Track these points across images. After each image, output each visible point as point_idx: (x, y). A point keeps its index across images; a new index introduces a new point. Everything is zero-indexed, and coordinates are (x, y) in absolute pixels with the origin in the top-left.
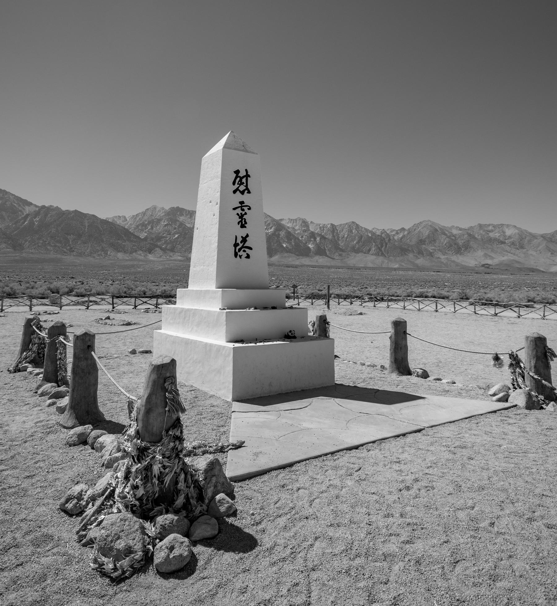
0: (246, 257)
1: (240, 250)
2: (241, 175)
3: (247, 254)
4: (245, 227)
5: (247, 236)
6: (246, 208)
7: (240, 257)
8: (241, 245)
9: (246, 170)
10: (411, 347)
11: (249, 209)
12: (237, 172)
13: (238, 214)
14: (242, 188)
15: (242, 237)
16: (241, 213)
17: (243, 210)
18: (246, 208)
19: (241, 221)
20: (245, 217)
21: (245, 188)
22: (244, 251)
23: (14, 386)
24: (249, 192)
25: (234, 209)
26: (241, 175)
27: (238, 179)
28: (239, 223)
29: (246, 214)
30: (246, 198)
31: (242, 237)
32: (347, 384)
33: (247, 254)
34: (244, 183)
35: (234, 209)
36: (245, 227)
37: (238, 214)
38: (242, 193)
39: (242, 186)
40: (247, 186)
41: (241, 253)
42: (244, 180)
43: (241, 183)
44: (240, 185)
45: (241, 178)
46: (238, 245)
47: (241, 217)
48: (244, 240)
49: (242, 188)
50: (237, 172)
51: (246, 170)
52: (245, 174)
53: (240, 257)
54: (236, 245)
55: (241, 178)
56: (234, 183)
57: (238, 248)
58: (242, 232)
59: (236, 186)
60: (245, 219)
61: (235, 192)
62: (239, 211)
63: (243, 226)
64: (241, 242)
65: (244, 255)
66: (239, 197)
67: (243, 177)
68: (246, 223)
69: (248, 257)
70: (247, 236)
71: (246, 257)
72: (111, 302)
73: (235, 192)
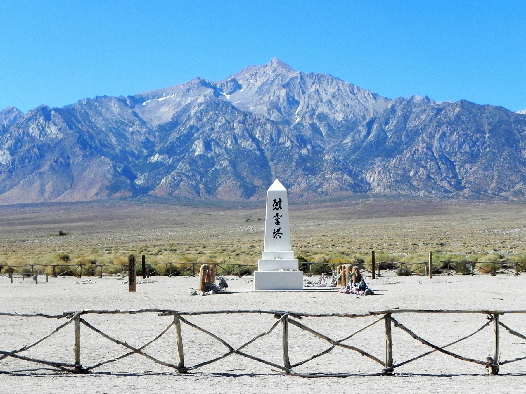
2: (277, 201)
12: (275, 200)
14: (277, 207)
23: (150, 253)
24: (281, 208)
26: (277, 201)
30: (280, 212)
38: (278, 209)
42: (278, 204)
43: (277, 205)
45: (277, 203)
47: (277, 220)
48: (278, 230)
49: (277, 207)
50: (275, 200)
54: (274, 233)
55: (277, 203)
56: (273, 206)
59: (275, 206)
61: (274, 209)
62: (276, 218)
63: (278, 224)
66: (276, 211)
69: (280, 238)
73: (274, 209)
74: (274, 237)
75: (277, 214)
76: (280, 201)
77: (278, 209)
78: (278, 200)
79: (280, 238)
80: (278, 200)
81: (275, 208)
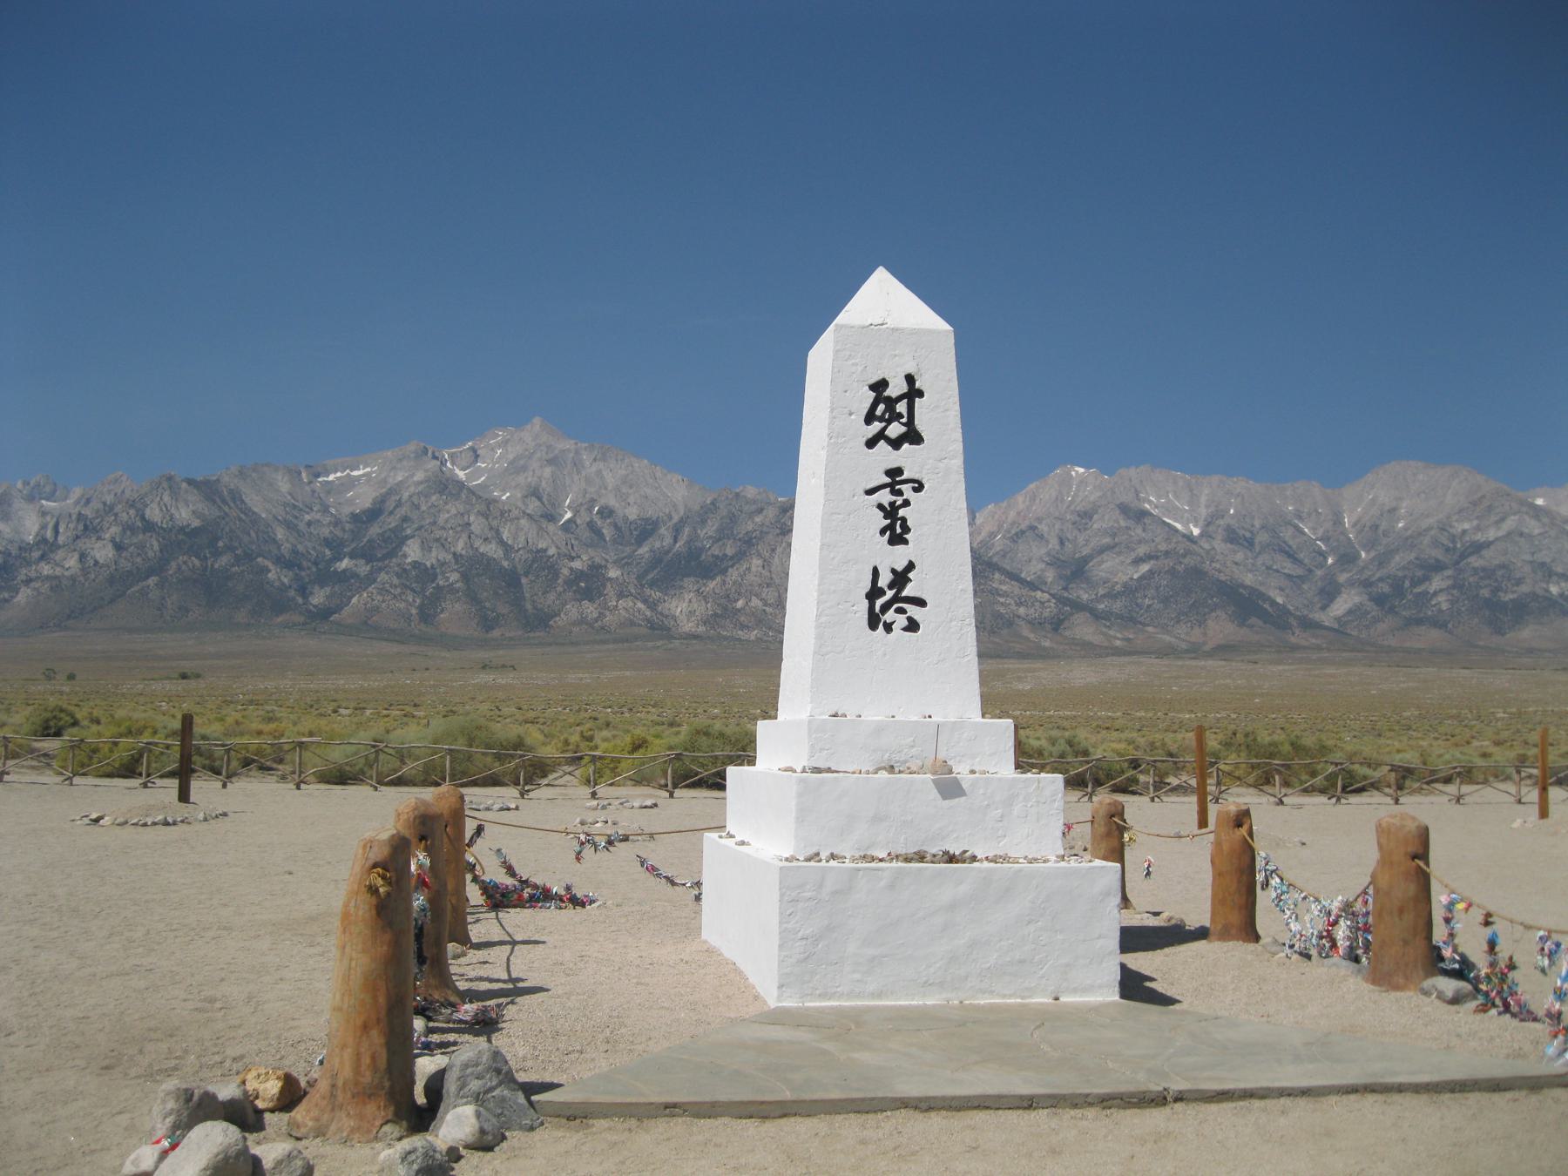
0: (905, 629)
1: (885, 608)
2: (893, 391)
3: (910, 619)
4: (906, 542)
5: (911, 566)
6: (905, 488)
7: (888, 628)
8: (890, 594)
9: (910, 379)
10: (1519, 1055)
11: (919, 487)
12: (880, 386)
13: (880, 507)
14: (895, 430)
15: (893, 571)
16: (892, 504)
17: (900, 493)
18: (905, 488)
19: (891, 527)
20: (901, 512)
21: (903, 429)
22: (901, 611)
25: (870, 492)
26: (893, 391)
27: (881, 407)
28: (883, 532)
29: (906, 503)
30: (907, 457)
31: (893, 571)
32: (720, 1121)
33: (910, 619)
34: (900, 416)
35: (870, 492)
36: (906, 542)
37: (880, 507)
39: (895, 424)
40: (910, 423)
41: (890, 616)
44: (889, 422)
46: (882, 593)
47: (890, 512)
49: (895, 430)
50: (880, 386)
51: (910, 379)
52: (904, 388)
53: (888, 628)
54: (874, 593)
55: (891, 403)
56: (870, 418)
57: (879, 603)
58: (898, 557)
59: (877, 426)
60: (904, 520)
61: (871, 443)
62: (885, 497)
64: (890, 587)
65: (901, 621)
66: (885, 456)
67: (900, 398)
68: (906, 529)
69: (912, 626)
70: (911, 566)
71: (905, 629)
72: (508, 947)
73: (871, 443)
74: (873, 621)
75: (894, 473)
76: (913, 393)
77: (896, 444)
78: (896, 388)
79: (912, 626)
80: (896, 388)
81: (881, 435)
